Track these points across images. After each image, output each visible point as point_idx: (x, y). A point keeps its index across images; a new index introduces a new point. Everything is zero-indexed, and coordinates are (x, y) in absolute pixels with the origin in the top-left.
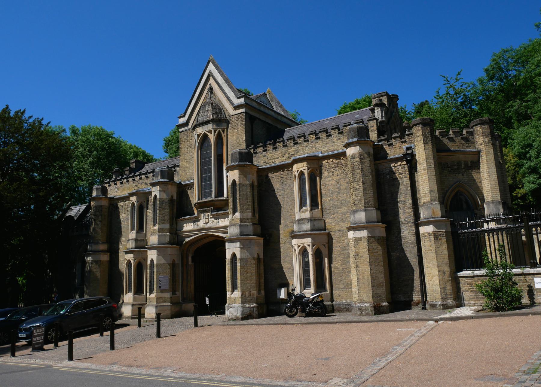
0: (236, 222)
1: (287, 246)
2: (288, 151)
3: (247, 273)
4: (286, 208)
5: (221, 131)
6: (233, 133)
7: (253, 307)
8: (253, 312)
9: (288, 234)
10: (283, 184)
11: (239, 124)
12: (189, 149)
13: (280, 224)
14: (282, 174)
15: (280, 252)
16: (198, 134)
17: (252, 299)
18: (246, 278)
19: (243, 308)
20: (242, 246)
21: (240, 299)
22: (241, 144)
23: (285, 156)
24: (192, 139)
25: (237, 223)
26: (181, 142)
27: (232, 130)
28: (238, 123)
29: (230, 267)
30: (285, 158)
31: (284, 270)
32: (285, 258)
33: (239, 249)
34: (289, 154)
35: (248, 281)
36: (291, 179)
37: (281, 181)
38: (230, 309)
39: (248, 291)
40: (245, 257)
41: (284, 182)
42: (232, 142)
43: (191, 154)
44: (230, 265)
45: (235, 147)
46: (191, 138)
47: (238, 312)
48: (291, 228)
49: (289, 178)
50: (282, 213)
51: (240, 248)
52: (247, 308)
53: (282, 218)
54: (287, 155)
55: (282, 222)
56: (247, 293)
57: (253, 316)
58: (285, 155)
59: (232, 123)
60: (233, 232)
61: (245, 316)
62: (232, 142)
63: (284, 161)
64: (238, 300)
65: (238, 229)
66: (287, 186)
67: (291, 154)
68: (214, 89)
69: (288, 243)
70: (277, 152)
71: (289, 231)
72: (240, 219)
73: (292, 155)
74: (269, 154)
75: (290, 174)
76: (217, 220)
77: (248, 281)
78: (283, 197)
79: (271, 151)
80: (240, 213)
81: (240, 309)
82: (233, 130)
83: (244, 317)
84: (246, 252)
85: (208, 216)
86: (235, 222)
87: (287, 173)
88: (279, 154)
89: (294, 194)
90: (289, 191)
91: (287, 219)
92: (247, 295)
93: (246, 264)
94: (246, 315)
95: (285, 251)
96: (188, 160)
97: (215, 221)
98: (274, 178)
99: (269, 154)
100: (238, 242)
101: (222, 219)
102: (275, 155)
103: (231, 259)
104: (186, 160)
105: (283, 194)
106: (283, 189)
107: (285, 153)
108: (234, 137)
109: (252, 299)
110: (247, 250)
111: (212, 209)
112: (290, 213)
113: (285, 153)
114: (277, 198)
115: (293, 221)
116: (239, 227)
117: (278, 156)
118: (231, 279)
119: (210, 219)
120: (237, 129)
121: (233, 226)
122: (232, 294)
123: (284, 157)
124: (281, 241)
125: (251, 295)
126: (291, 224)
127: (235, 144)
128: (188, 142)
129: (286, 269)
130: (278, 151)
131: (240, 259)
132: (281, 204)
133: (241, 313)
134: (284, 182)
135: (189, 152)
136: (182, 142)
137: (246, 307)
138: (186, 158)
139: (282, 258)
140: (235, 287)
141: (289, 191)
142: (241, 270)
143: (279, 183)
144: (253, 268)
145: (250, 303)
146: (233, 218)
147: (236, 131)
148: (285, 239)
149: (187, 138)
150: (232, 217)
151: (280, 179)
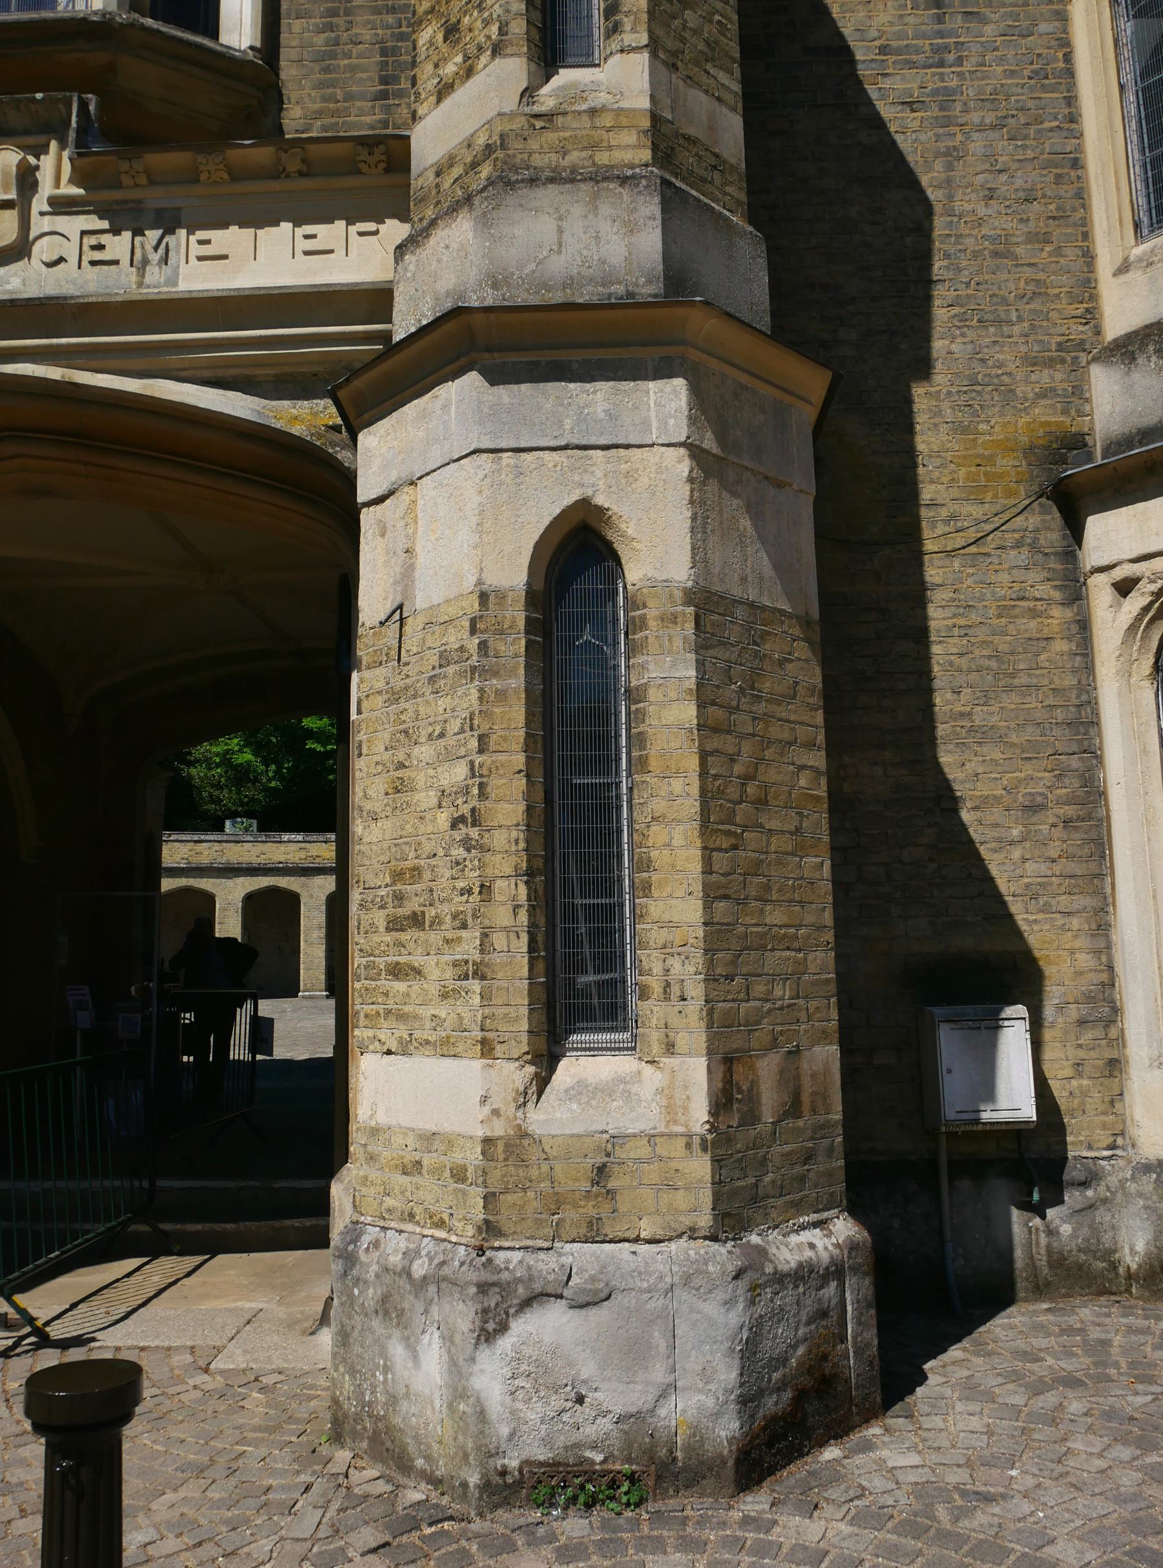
0: (594, 146)
1: (1004, 577)
3: (761, 802)
4: (980, 221)
7: (836, 1272)
8: (843, 1339)
9: (1007, 463)
13: (923, 367)
15: (921, 635)
17: (809, 1157)
18: (755, 869)
19: (754, 1290)
20: (709, 442)
21: (701, 1167)
25: (603, 158)
29: (517, 713)
31: (966, 816)
32: (986, 698)
33: (680, 465)
35: (775, 916)
38: (523, 1327)
39: (774, 1044)
40: (737, 592)
44: (517, 682)
47: (691, 1363)
48: (1046, 414)
50: (938, 266)
51: (695, 451)
52: (789, 1296)
53: (940, 314)
55: (939, 345)
56: (767, 1068)
57: (847, 1381)
60: (559, 265)
61: (771, 1404)
64: (652, 1173)
65: (631, 228)
66: (989, 29)
69: (1021, 556)
71: (1024, 439)
72: (655, 118)
76: (153, 235)
77: (775, 916)
78: (947, 122)
80: (653, 46)
81: (711, 1308)
83: (773, 1420)
84: (746, 523)
85: (27, 180)
86: (574, 157)
89: (1071, 100)
91: (999, 322)
92: (769, 1101)
93: (750, 687)
94: (788, 1395)
95: (981, 634)
97: (119, 245)
100: (662, 371)
101: (224, 225)
103: (532, 598)
105: (949, 92)
106: (946, 48)
109: (809, 1157)
110: (754, 510)
111: (83, 105)
112: (1028, 272)
114: (878, 124)
115: (1060, 347)
116: (650, 208)
118: (530, 873)
119: (39, 224)
121: (548, 195)
122: (542, 1082)
124: (926, 533)
125: (806, 1099)
126: (1044, 377)
129: (996, 814)
131: (690, 596)
132: (924, 180)
133: (728, 1374)
137: (780, 1279)
139: (941, 700)
140: (571, 983)
141: (1012, 74)
142: (704, 756)
144: (810, 745)
145: (798, 1207)
146: (548, 96)
148: (977, 511)
150: (528, 94)
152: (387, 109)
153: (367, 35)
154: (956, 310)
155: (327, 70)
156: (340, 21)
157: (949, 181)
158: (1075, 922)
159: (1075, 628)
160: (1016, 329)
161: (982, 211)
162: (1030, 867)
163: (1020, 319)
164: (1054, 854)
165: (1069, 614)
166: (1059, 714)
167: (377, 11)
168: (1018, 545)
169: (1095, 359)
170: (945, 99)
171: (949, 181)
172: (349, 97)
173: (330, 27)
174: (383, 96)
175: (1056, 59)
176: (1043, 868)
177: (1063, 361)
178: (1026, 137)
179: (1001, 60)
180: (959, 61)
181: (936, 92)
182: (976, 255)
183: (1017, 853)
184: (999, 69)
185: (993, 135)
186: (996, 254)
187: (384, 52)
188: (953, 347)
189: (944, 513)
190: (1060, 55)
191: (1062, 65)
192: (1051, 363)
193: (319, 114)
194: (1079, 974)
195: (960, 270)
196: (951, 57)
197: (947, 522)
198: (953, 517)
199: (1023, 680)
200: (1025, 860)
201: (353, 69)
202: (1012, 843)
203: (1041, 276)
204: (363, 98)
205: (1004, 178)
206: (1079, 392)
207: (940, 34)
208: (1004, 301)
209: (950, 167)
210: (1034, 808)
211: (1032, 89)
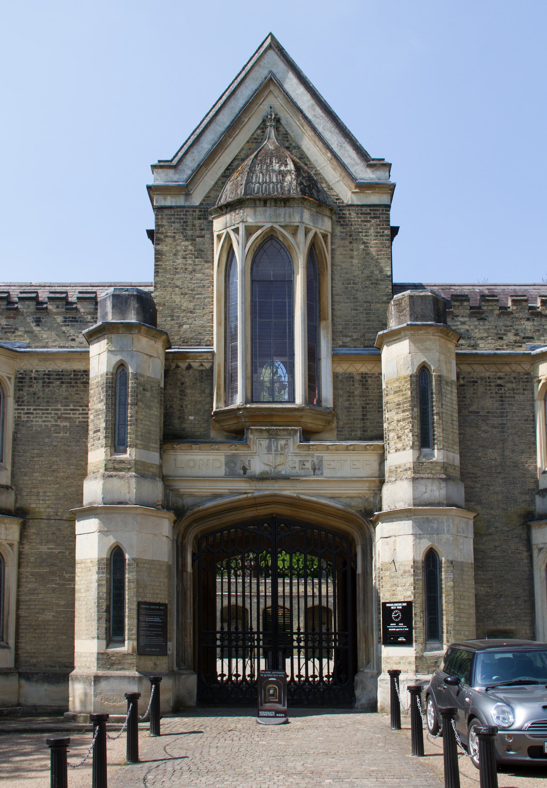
2: (515, 327)
5: (320, 236)
6: (352, 250)
10: (502, 401)
11: (372, 231)
12: (189, 261)
14: (500, 378)
16: (247, 224)
22: (377, 284)
23: (505, 337)
24: (203, 237)
26: (162, 237)
27: (347, 243)
28: (370, 229)
30: (505, 342)
34: (517, 335)
36: (526, 392)
37: (496, 393)
41: (505, 397)
42: (347, 273)
43: (199, 276)
45: (359, 286)
46: (198, 233)
49: (521, 391)
54: (511, 337)
58: (505, 334)
59: (347, 225)
62: (347, 273)
63: (503, 349)
66: (514, 408)
67: (522, 335)
68: (283, 122)
70: (481, 323)
73: (524, 338)
74: (459, 323)
75: (523, 382)
79: (467, 319)
82: (351, 243)
87: (515, 378)
88: (489, 329)
90: (519, 420)
96: (186, 291)
98: (476, 382)
99: (459, 323)
102: (476, 331)
104: (177, 287)
105: (505, 424)
106: (503, 413)
107: (505, 330)
108: (355, 261)
113: (505, 330)
117: (486, 335)
120: (364, 243)
123: (501, 338)
127: (357, 280)
128: (187, 240)
130: (486, 323)
134: (505, 397)
135: (190, 268)
136: (166, 237)
138: (179, 283)
141: (519, 420)
143: (491, 397)
147: (362, 247)
149: (185, 229)
151: (495, 389)
152: (364, 423)
153: (358, 403)
154: (504, 480)
155: (348, 412)
156: (351, 399)
157: (503, 447)
158: (526, 623)
159: (529, 557)
160: (518, 485)
161: (511, 455)
162: (516, 611)
163: (519, 483)
164: (522, 608)
165: (528, 554)
166: (524, 577)
167: (361, 396)
168: (516, 537)
169: (536, 494)
170: (503, 425)
171: (503, 447)
172: (354, 419)
173: (349, 400)
174: (363, 419)
175: (530, 417)
176: (519, 611)
177: (529, 493)
178: (522, 437)
179: (517, 416)
180: (507, 416)
181: (501, 424)
182: (509, 466)
183: (513, 608)
184: (517, 419)
185: (514, 436)
186: (514, 466)
187: (363, 408)
188: (503, 489)
189: (499, 529)
190: (531, 415)
191: (532, 418)
192: (526, 494)
193: (347, 423)
194: (526, 634)
195: (505, 470)
196: (505, 415)
197: (500, 532)
198: (501, 530)
199: (516, 568)
200: (515, 609)
201: (355, 412)
202: (513, 605)
203: (525, 472)
204: (358, 419)
205: (517, 447)
206: (533, 501)
207: (502, 409)
208: (515, 478)
209: (503, 444)
210: (518, 598)
211: (525, 424)
